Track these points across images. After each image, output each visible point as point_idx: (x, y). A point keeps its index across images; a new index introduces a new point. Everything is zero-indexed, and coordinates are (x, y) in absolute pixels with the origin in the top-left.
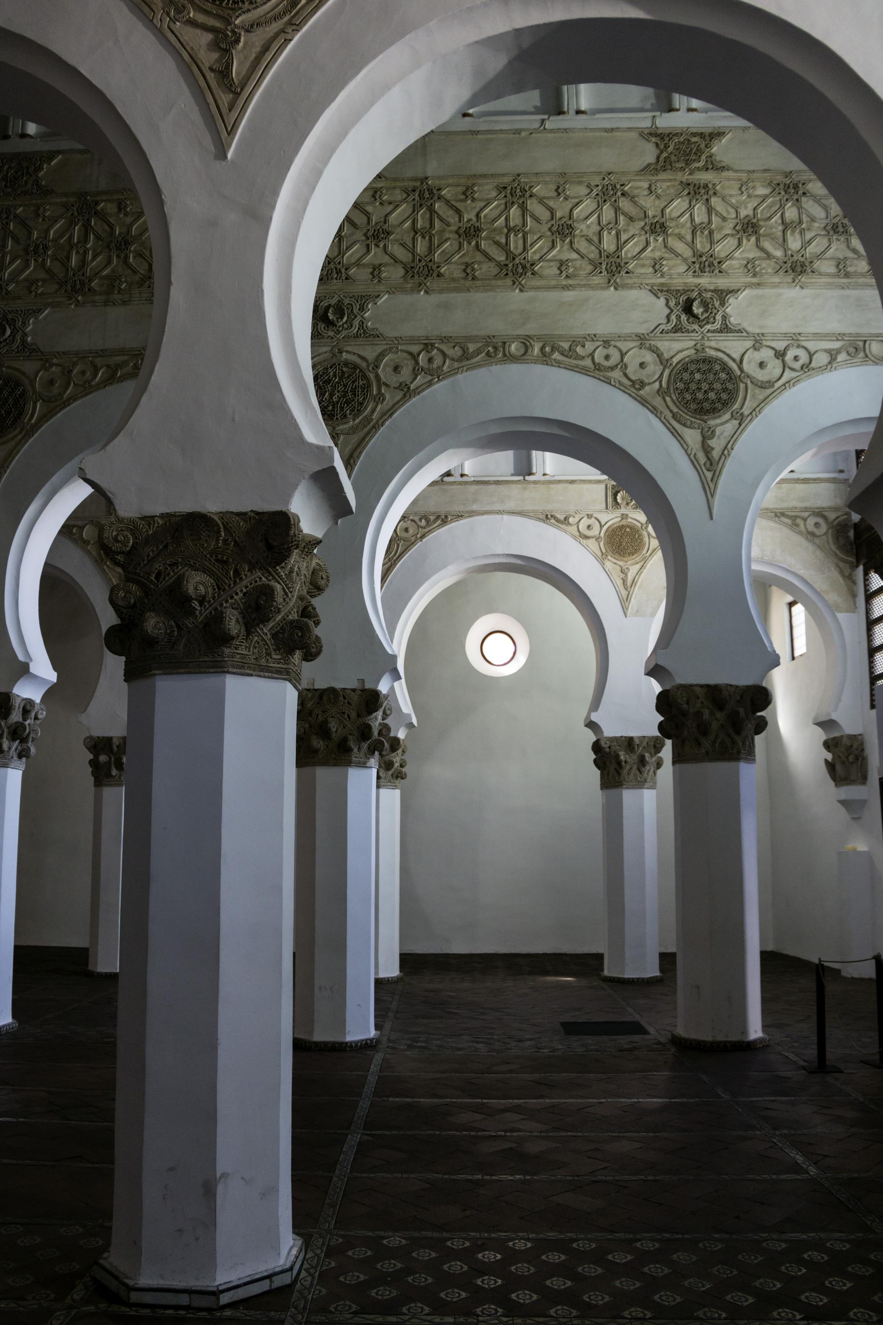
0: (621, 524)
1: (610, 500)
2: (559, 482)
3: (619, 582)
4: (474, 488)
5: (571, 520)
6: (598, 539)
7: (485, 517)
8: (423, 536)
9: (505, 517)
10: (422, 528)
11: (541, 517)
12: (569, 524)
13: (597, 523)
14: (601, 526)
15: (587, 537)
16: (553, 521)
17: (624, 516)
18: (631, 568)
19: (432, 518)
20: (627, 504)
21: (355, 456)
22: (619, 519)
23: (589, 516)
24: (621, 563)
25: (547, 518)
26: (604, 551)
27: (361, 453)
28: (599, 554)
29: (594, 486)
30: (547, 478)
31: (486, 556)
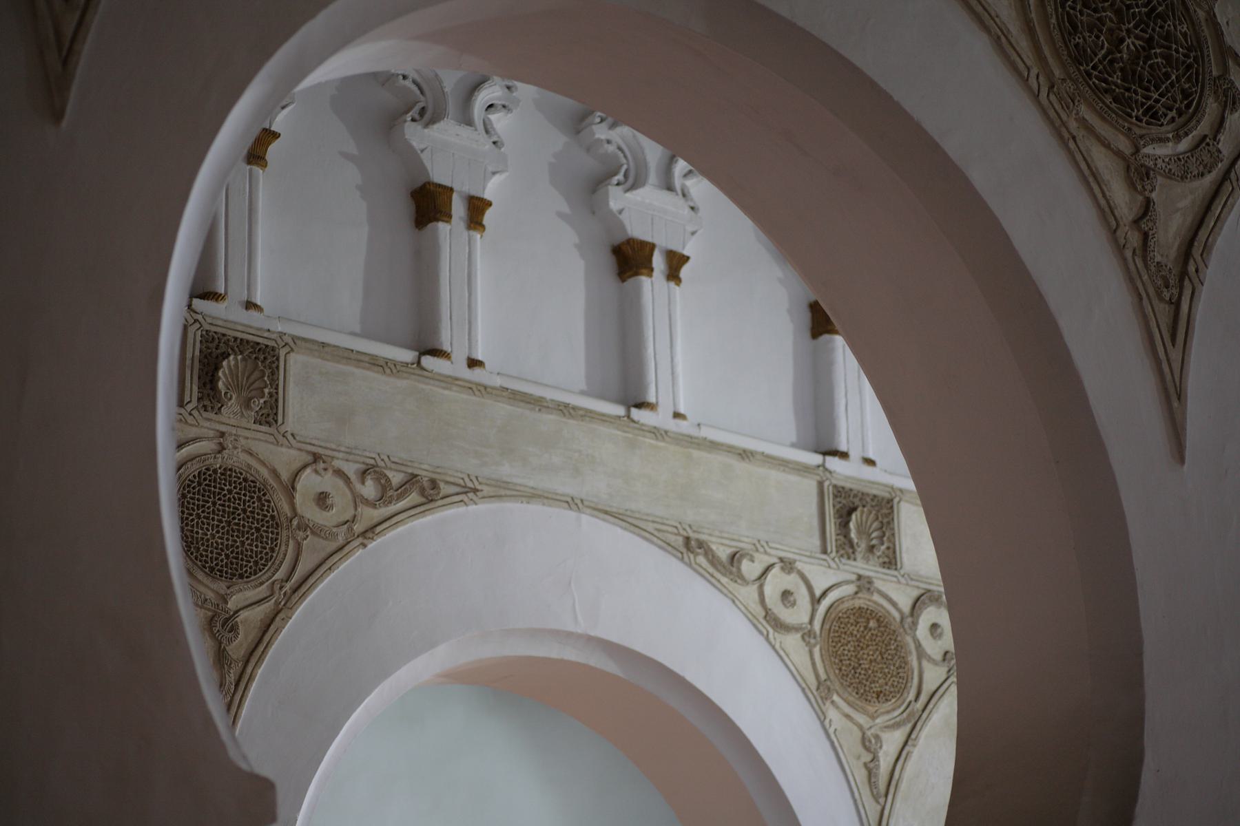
0: (858, 603)
1: (831, 528)
2: (714, 446)
3: (860, 775)
4: (502, 410)
5: (746, 566)
6: (807, 635)
7: (535, 508)
8: (370, 532)
9: (587, 521)
10: (367, 502)
11: (672, 539)
12: (739, 578)
13: (803, 590)
14: (816, 601)
15: (780, 626)
16: (701, 560)
17: (864, 584)
18: (885, 736)
19: (396, 478)
20: (871, 549)
21: (1196, 252)
22: (851, 589)
23: (788, 566)
24: (862, 719)
25: (691, 547)
26: (823, 676)
27: (1207, 248)
28: (813, 682)
29: (793, 478)
30: (683, 427)
31: (536, 634)
